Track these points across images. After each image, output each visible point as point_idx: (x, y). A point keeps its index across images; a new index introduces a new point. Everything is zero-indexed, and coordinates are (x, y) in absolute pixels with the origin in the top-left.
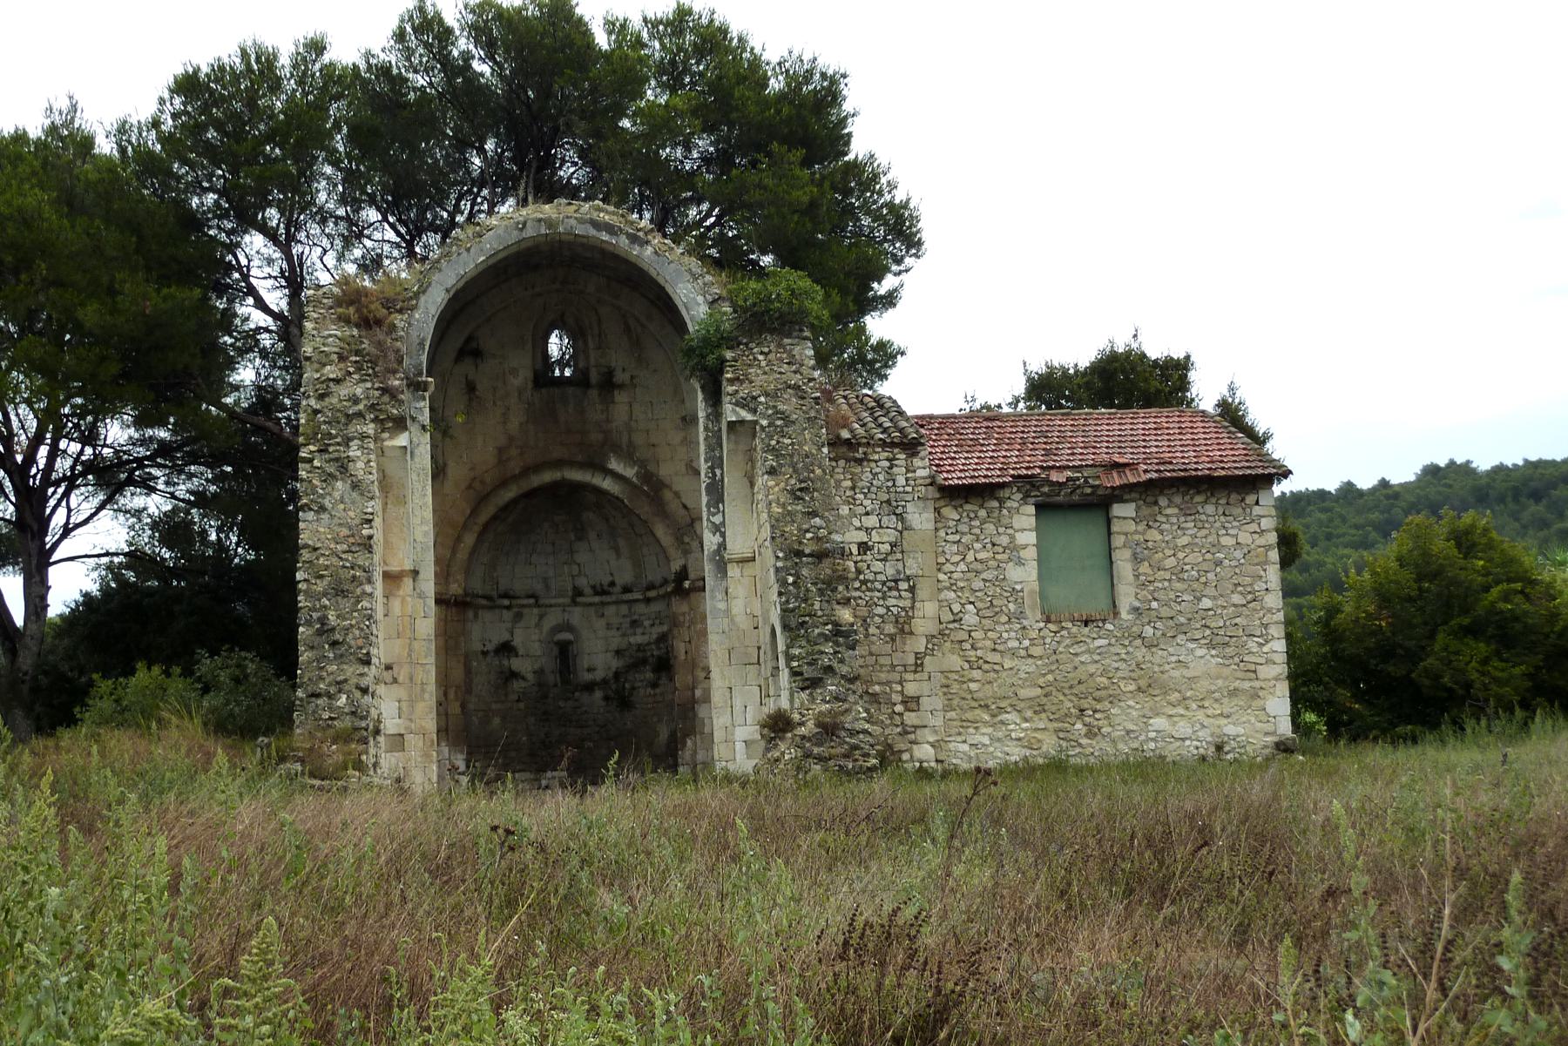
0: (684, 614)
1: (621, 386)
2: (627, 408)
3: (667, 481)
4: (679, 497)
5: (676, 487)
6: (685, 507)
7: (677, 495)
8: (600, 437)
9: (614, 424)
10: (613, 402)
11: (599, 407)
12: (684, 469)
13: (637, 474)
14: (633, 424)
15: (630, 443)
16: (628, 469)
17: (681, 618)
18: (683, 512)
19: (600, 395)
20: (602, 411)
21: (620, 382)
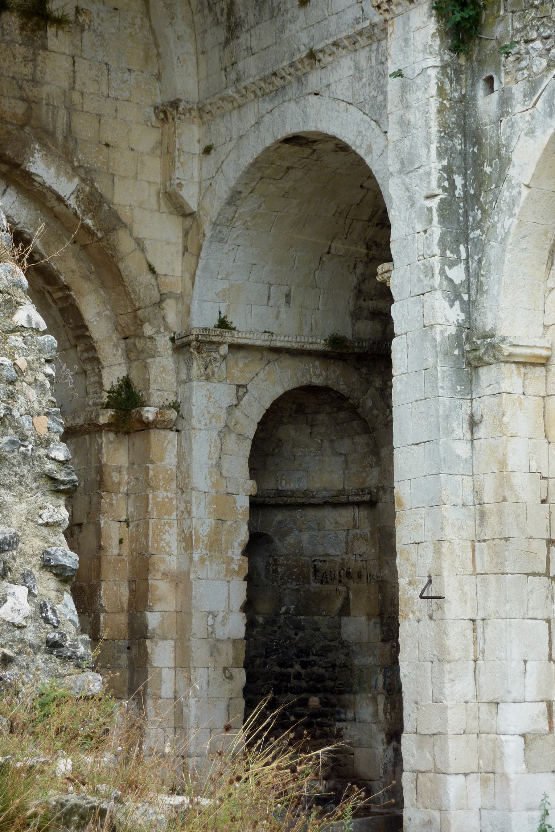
0: (119, 470)
1: (60, 22)
2: (67, 64)
3: (125, 215)
4: (143, 250)
5: (140, 231)
6: (152, 270)
7: (139, 243)
8: (20, 108)
9: (46, 89)
10: (45, 48)
11: (20, 50)
12: (153, 200)
13: (78, 192)
14: (76, 96)
15: (70, 131)
16: (63, 179)
17: (115, 477)
18: (147, 277)
19: (22, 28)
20: (25, 59)
21: (57, 14)
